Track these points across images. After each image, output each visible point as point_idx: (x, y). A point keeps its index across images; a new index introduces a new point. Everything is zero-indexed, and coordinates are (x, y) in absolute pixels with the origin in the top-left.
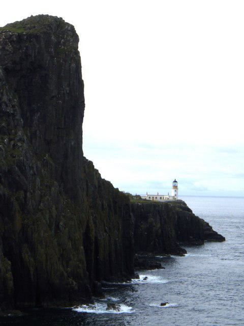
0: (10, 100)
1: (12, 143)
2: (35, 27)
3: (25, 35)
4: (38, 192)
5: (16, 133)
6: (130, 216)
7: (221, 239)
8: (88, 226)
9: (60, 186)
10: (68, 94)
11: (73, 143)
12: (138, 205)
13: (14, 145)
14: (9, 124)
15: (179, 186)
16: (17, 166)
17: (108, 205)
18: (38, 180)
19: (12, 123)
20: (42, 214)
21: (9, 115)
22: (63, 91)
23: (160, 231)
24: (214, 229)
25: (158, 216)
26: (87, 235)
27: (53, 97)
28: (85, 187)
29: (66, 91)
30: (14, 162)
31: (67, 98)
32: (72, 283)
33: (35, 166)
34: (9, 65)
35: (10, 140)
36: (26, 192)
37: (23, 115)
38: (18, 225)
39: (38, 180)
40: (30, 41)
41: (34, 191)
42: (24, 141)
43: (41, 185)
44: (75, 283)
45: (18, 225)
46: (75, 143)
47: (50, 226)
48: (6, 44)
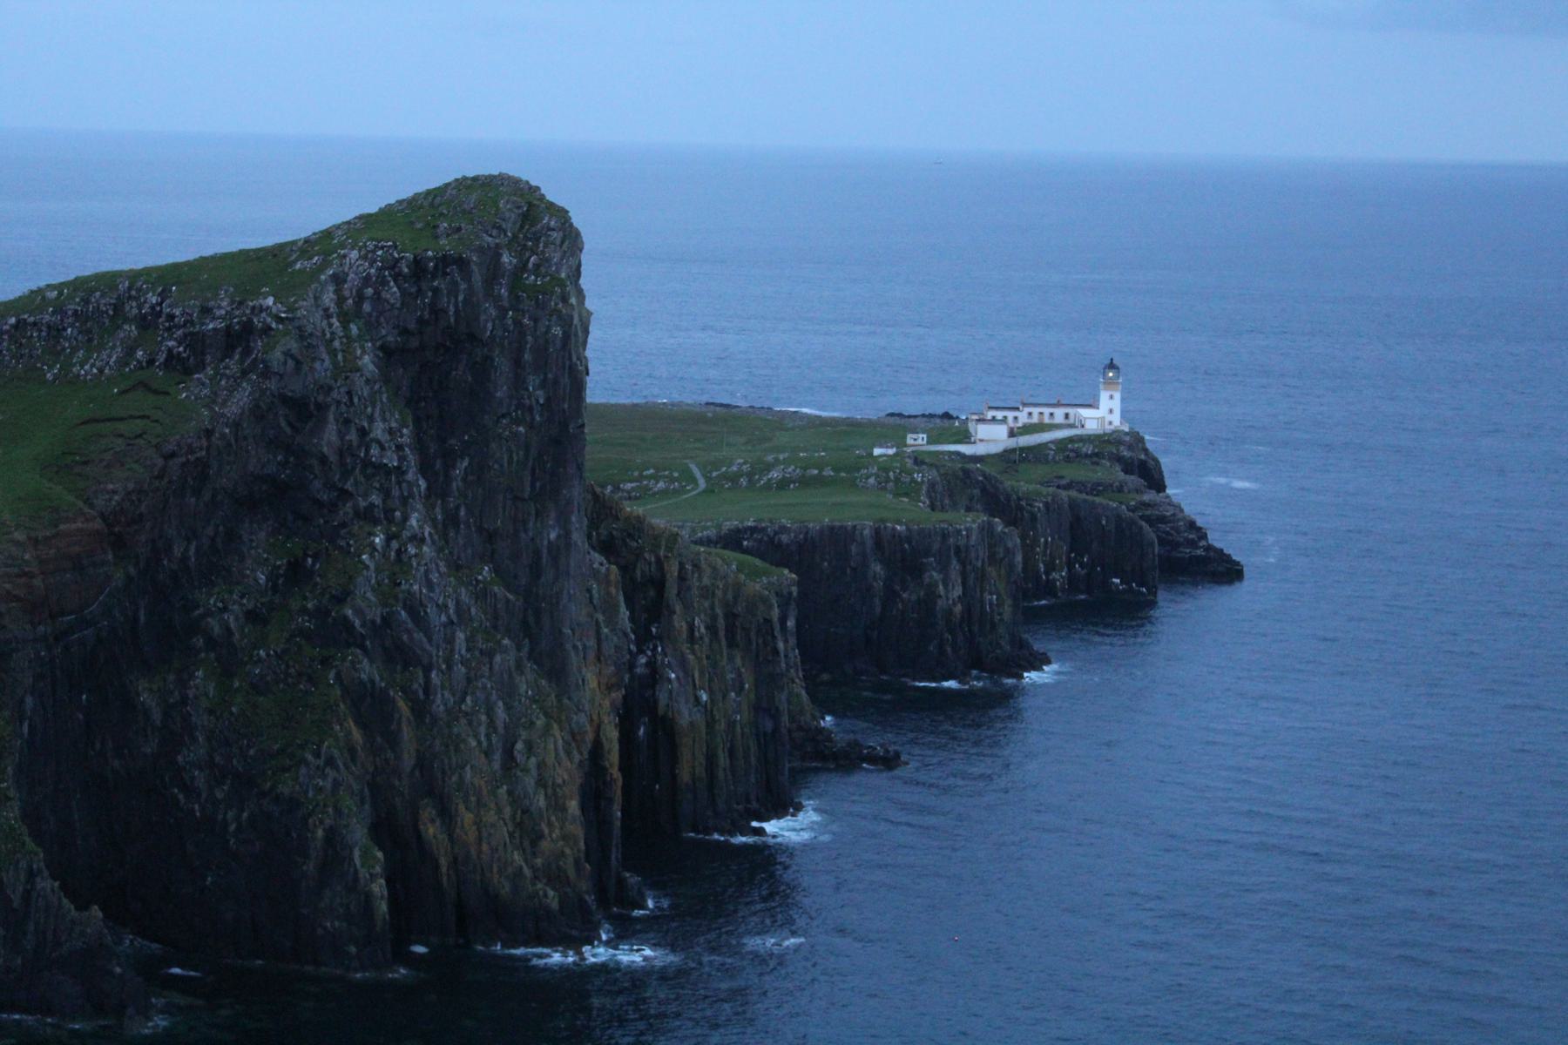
0: (391, 431)
1: (395, 545)
2: (459, 229)
3: (430, 259)
5: (405, 518)
7: (1225, 571)
9: (519, 648)
11: (553, 536)
12: (894, 529)
13: (399, 552)
14: (387, 494)
16: (404, 608)
17: (707, 628)
19: (396, 492)
20: (470, 723)
21: (388, 471)
23: (958, 608)
25: (955, 565)
28: (592, 643)
30: (396, 598)
31: (538, 418)
32: (546, 895)
34: (390, 338)
35: (389, 539)
36: (427, 670)
37: (425, 469)
41: (450, 668)
42: (423, 540)
43: (468, 650)
44: (551, 893)
46: (559, 536)
48: (384, 283)
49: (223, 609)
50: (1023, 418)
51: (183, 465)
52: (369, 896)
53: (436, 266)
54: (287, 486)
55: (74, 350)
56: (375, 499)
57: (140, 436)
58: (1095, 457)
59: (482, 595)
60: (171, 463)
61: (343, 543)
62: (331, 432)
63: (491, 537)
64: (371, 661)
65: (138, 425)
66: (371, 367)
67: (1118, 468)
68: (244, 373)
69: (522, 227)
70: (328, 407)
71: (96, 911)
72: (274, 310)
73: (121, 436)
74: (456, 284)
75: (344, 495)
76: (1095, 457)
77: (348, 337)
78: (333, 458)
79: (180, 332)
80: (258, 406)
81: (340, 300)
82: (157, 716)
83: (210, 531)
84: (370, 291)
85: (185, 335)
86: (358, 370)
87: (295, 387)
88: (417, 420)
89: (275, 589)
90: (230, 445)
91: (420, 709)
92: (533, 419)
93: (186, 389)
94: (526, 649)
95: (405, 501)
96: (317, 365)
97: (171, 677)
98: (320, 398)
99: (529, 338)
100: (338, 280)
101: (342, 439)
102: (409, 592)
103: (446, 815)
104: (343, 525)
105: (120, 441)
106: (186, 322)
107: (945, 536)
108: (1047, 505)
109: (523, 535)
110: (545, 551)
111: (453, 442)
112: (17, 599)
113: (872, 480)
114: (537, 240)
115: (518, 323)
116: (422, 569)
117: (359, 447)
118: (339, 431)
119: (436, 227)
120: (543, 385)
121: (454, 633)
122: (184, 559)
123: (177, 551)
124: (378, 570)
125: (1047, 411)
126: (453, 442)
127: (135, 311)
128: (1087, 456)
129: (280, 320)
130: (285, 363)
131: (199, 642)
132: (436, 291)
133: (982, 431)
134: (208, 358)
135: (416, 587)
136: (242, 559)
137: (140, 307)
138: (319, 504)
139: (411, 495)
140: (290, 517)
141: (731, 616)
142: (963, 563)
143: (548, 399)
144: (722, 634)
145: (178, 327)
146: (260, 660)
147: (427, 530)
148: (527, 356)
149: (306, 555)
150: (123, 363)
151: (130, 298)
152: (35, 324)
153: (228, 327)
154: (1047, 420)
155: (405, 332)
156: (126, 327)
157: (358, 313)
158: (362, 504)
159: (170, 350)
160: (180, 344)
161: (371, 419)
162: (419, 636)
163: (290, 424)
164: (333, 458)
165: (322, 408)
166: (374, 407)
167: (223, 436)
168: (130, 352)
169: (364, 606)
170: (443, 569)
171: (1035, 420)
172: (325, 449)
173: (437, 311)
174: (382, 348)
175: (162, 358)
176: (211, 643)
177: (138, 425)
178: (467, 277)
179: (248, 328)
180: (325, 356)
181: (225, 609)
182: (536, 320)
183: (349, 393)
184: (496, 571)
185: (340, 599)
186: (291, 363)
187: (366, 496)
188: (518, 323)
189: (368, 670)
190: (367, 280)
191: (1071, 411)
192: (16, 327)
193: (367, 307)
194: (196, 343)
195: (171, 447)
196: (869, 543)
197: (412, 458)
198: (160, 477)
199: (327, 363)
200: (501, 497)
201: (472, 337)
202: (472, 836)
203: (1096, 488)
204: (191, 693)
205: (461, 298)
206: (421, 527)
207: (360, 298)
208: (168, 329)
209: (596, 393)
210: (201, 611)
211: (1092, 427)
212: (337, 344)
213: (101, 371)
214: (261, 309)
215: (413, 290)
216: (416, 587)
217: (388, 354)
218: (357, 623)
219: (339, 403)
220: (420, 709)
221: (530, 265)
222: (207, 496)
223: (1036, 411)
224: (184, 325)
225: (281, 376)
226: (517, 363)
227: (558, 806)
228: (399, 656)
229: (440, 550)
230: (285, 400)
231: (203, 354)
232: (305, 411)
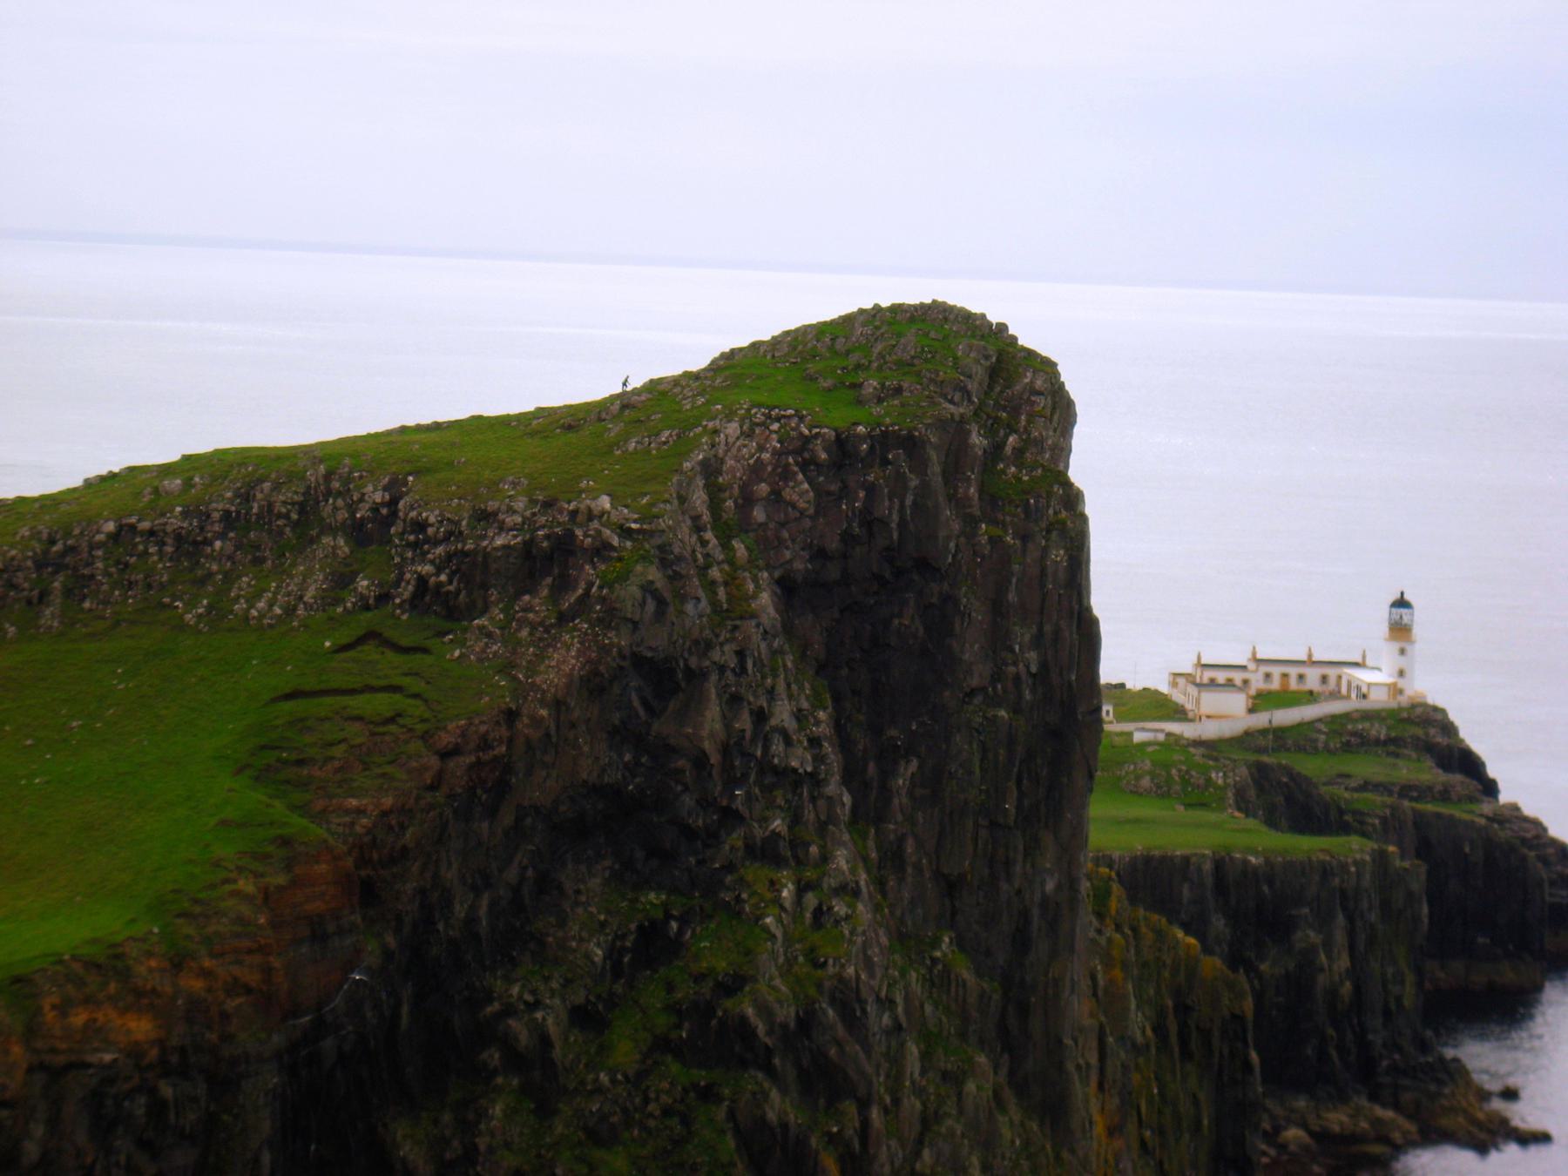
0: (799, 715)
1: (811, 900)
2: (898, 391)
5: (825, 858)
6: (1247, 1066)
9: (996, 1068)
10: (1034, 676)
11: (1050, 886)
12: (1245, 862)
13: (818, 912)
14: (795, 820)
15: (1421, 619)
16: (833, 1001)
18: (913, 1049)
19: (809, 814)
21: (786, 775)
22: (1015, 664)
23: (1347, 988)
25: (1341, 919)
27: (972, 693)
28: (1094, 1060)
29: (1028, 667)
31: (1028, 695)
33: (899, 1000)
34: (798, 565)
35: (802, 889)
36: (864, 1105)
37: (851, 776)
39: (913, 1049)
40: (885, 462)
41: (896, 1101)
42: (856, 893)
43: (923, 1072)
46: (1059, 887)
48: (786, 475)
49: (538, 1006)
50: (1257, 683)
51: (471, 767)
53: (872, 447)
54: (637, 802)
55: (230, 578)
56: (777, 824)
57: (391, 720)
58: (1392, 745)
59: (940, 980)
60: (451, 764)
61: (727, 897)
62: (711, 719)
64: (784, 1091)
65: (380, 704)
66: (771, 611)
67: (1429, 763)
68: (563, 619)
69: (991, 387)
70: (703, 675)
72: (614, 518)
73: (359, 718)
74: (900, 477)
75: (730, 816)
76: (1392, 745)
77: (731, 561)
78: (715, 758)
79: (440, 550)
80: (597, 673)
81: (715, 505)
83: (512, 875)
84: (763, 488)
85: (449, 557)
86: (753, 616)
87: (657, 641)
88: (837, 699)
89: (617, 971)
90: (548, 735)
92: (1020, 696)
93: (462, 643)
94: (1004, 1071)
95: (822, 827)
96: (689, 607)
97: (447, 1117)
98: (693, 662)
99: (1016, 567)
100: (710, 469)
101: (728, 727)
102: (840, 978)
104: (730, 867)
105: (356, 727)
106: (449, 534)
107: (1326, 871)
108: (1384, 820)
109: (1004, 886)
110: (1035, 912)
111: (893, 732)
112: (248, 990)
113: (1146, 782)
114: (1015, 412)
116: (860, 940)
117: (753, 740)
118: (724, 717)
119: (856, 386)
120: (1037, 641)
121: (902, 1045)
122: (471, 920)
123: (460, 910)
124: (788, 940)
125: (1293, 672)
126: (893, 732)
127: (343, 515)
128: (1377, 742)
129: (625, 532)
130: (643, 604)
131: (493, 1056)
132: (871, 489)
133: (1211, 702)
134: (494, 594)
135: (851, 970)
136: (562, 923)
137: (352, 508)
138: (689, 833)
139: (832, 819)
140: (639, 854)
141: (1183, 1009)
142: (1350, 919)
143: (1044, 665)
144: (1174, 1039)
145: (436, 542)
146: (599, 1090)
147: (863, 877)
148: (1012, 597)
149: (668, 916)
150: (329, 599)
151: (329, 493)
152: (152, 533)
153: (529, 545)
154: (1293, 685)
155: (820, 554)
156: (327, 540)
157: (746, 525)
158: (759, 833)
159: (422, 581)
160: (439, 571)
161: (771, 692)
162: (854, 1048)
163: (645, 703)
164: (715, 758)
165: (696, 677)
166: (775, 676)
167: (536, 721)
169: (770, 999)
170: (884, 940)
171: (1275, 685)
172: (707, 745)
173: (870, 522)
174: (780, 582)
175: (407, 591)
176: (515, 1060)
177: (380, 704)
178: (920, 465)
179: (564, 546)
180: (701, 593)
181: (537, 1005)
182: (1025, 538)
183: (741, 654)
184: (960, 943)
185: (734, 984)
186: (651, 606)
187: (764, 820)
188: (995, 541)
189: (779, 1106)
190: (756, 471)
191: (1332, 672)
192: (115, 537)
193: (759, 514)
194: (474, 571)
195: (446, 739)
196: (1209, 881)
198: (432, 788)
199: (704, 603)
200: (970, 824)
201: (925, 565)
203: (1406, 790)
204: (482, 1143)
205: (909, 500)
206: (853, 871)
207: (747, 500)
208: (415, 546)
209: (1132, 654)
210: (495, 1007)
211: (1379, 699)
212: (715, 573)
213: (290, 611)
214: (591, 516)
215: (834, 487)
216: (851, 970)
217: (787, 588)
218: (761, 1029)
219: (722, 669)
221: (1008, 450)
222: (507, 818)
223: (1276, 671)
224: (446, 539)
225: (636, 625)
226: (998, 608)
228: (824, 1082)
229: (877, 908)
230: (638, 661)
231: (485, 586)
232: (667, 679)
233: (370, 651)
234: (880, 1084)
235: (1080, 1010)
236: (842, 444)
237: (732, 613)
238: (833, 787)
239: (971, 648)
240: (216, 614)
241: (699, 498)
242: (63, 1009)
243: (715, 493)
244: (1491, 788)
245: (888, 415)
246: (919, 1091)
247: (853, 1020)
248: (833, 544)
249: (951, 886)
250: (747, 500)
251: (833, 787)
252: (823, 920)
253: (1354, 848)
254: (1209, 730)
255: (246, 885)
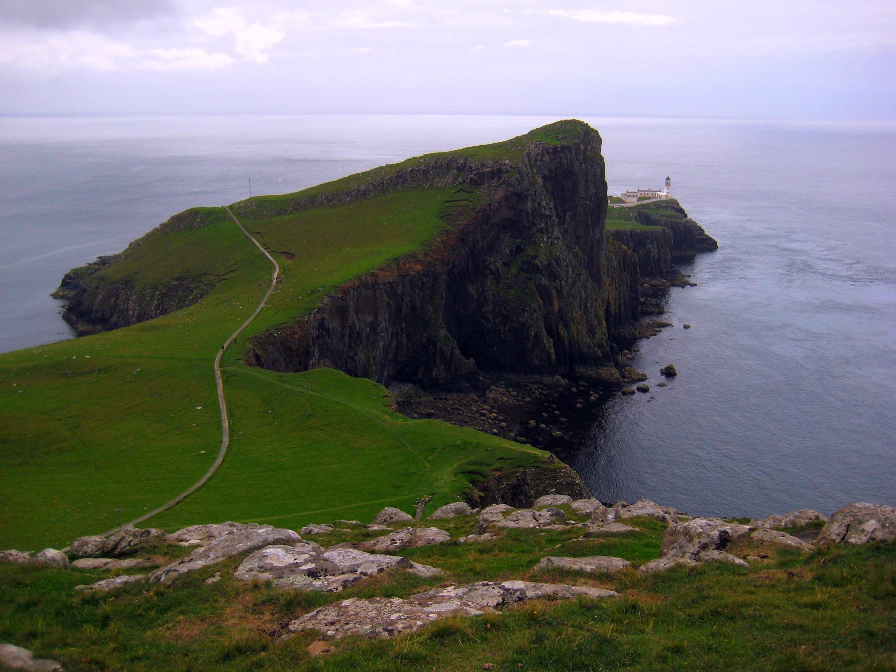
1: (550, 240)
4: (570, 280)
8: (608, 303)
14: (547, 224)
15: (672, 181)
21: (545, 216)
24: (706, 233)
26: (607, 312)
35: (548, 238)
36: (561, 280)
37: (557, 215)
38: (556, 308)
45: (556, 308)
47: (580, 307)
48: (544, 155)
49: (496, 262)
50: (639, 195)
52: (549, 355)
58: (666, 207)
59: (576, 256)
62: (529, 205)
63: (578, 237)
65: (464, 203)
68: (500, 185)
71: (472, 359)
76: (666, 207)
81: (529, 162)
82: (475, 297)
84: (539, 158)
91: (559, 292)
95: (552, 225)
100: (528, 154)
103: (567, 326)
107: (652, 233)
115: (586, 168)
129: (512, 168)
131: (488, 272)
133: (630, 199)
141: (624, 261)
150: (453, 183)
155: (551, 171)
168: (456, 178)
169: (542, 260)
173: (561, 165)
175: (468, 180)
176: (492, 273)
184: (580, 248)
185: (535, 257)
188: (586, 168)
189: (544, 281)
190: (538, 155)
193: (538, 163)
194: (482, 176)
195: (477, 210)
197: (554, 212)
201: (571, 173)
202: (575, 334)
207: (536, 161)
211: (663, 198)
217: (544, 178)
220: (559, 292)
226: (586, 181)
227: (600, 323)
228: (553, 276)
230: (515, 193)
232: (521, 197)
233: (462, 193)
234: (564, 276)
235: (604, 261)
236: (555, 149)
237: (533, 183)
238: (554, 218)
239: (581, 189)
240: (431, 186)
241: (526, 161)
242: (404, 264)
243: (529, 158)
244: (686, 216)
245: (564, 143)
246: (572, 277)
247: (559, 264)
248: (553, 169)
249: (578, 237)
250: (536, 161)
251: (554, 218)
252: (553, 245)
253: (658, 228)
254: (629, 205)
255: (439, 239)
